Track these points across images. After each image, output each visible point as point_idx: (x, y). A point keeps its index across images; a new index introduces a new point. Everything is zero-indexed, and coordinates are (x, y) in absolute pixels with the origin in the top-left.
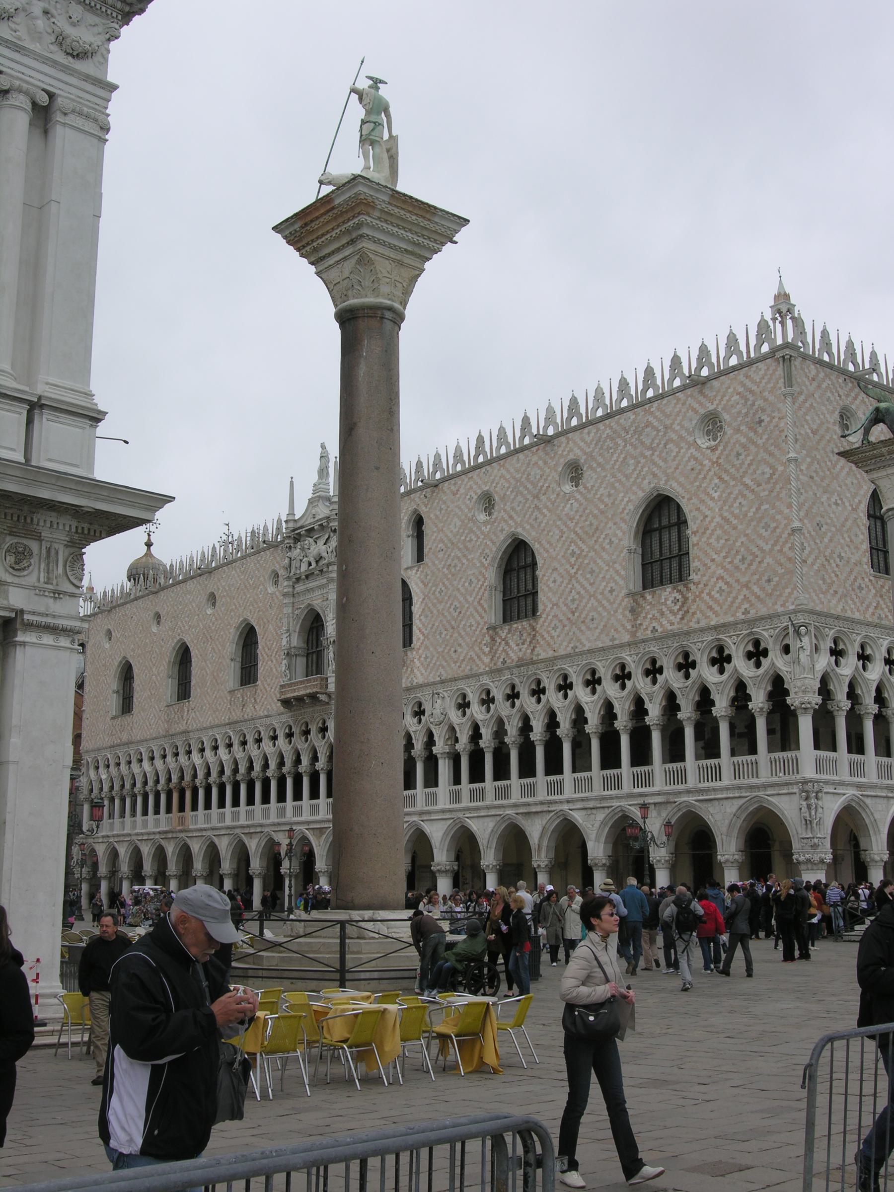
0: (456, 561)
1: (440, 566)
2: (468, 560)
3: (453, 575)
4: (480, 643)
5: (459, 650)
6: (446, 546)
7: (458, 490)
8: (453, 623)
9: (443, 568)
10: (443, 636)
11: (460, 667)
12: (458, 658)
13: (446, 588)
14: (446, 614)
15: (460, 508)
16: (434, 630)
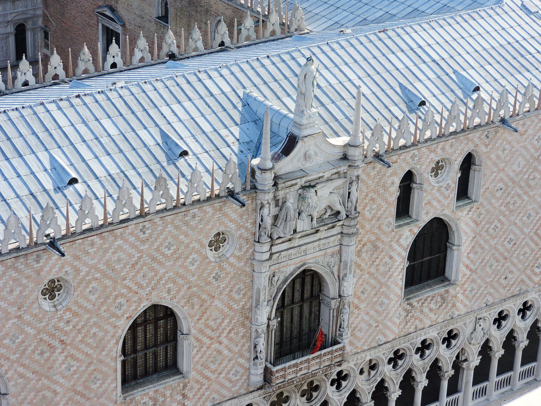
0: (516, 198)
1: (497, 205)
2: (529, 196)
3: (511, 211)
4: (533, 266)
5: (510, 276)
6: (506, 185)
7: (526, 131)
8: (506, 254)
9: (501, 205)
10: (493, 267)
11: (508, 290)
12: (508, 284)
13: (502, 224)
14: (499, 247)
15: (525, 148)
16: (483, 264)
